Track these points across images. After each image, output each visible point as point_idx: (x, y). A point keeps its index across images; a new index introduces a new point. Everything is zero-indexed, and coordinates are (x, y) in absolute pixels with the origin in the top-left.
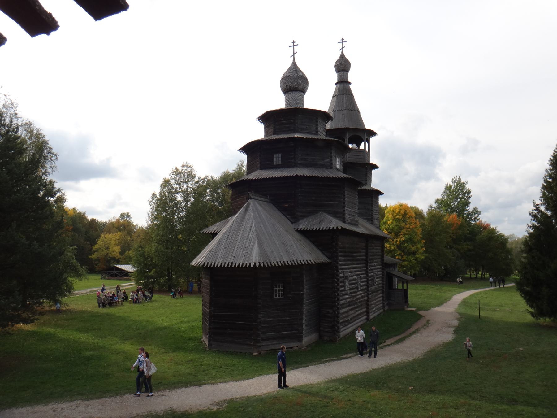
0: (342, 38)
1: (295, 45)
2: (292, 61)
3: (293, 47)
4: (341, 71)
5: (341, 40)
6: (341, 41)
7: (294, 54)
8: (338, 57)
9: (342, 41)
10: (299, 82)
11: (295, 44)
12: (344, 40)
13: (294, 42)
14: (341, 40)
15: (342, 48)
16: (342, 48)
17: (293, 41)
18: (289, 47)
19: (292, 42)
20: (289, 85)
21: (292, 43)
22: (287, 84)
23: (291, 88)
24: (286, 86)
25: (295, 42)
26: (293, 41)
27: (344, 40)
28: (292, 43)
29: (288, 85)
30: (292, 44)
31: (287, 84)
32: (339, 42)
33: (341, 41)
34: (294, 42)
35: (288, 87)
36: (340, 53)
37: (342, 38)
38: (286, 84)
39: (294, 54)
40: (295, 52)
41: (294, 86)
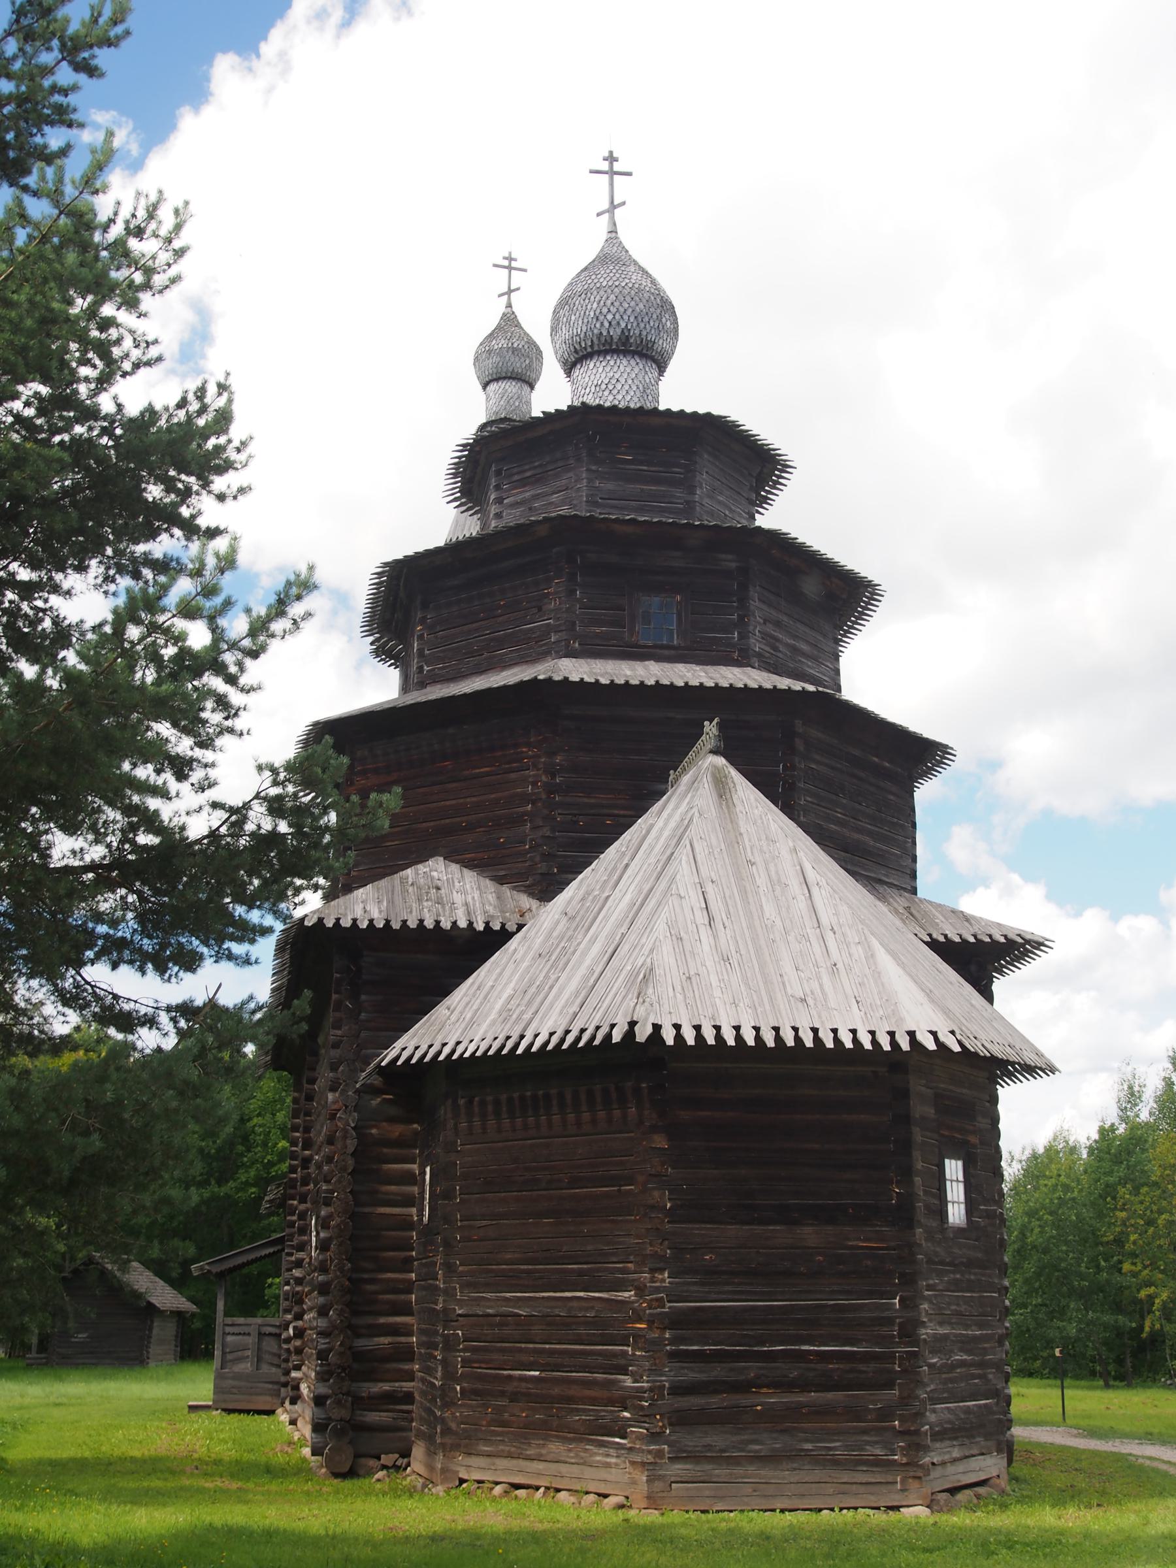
0: (510, 253)
1: (615, 169)
2: (604, 236)
3: (606, 176)
4: (514, 379)
5: (505, 258)
6: (506, 263)
7: (613, 207)
8: (491, 321)
9: (509, 265)
10: (664, 320)
11: (617, 167)
12: (515, 260)
13: (611, 158)
14: (505, 258)
15: (510, 291)
16: (510, 291)
17: (611, 153)
18: (592, 172)
19: (607, 155)
20: (623, 325)
21: (605, 159)
22: (617, 316)
23: (628, 338)
24: (606, 324)
25: (616, 160)
26: (611, 153)
27: (515, 260)
28: (605, 159)
29: (618, 323)
30: (605, 166)
31: (617, 316)
32: (495, 266)
33: (506, 263)
34: (611, 158)
35: (619, 331)
36: (500, 307)
37: (510, 253)
38: (610, 317)
39: (613, 207)
40: (616, 203)
41: (644, 333)
